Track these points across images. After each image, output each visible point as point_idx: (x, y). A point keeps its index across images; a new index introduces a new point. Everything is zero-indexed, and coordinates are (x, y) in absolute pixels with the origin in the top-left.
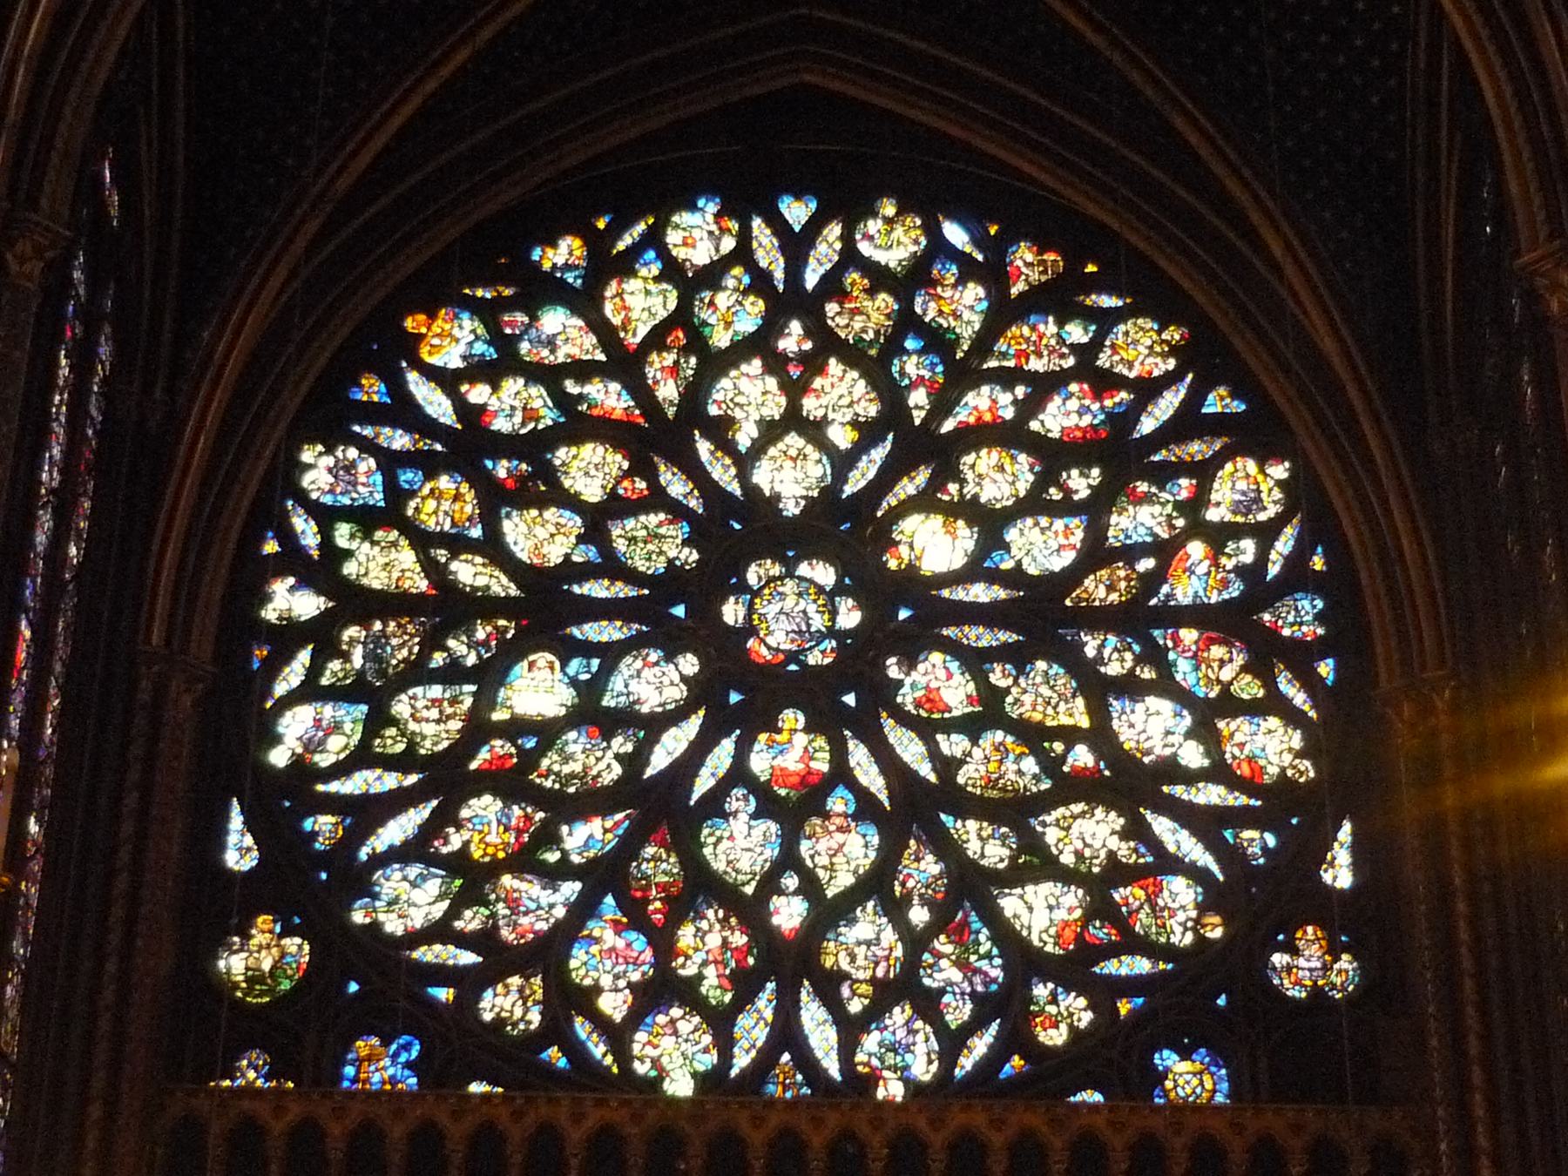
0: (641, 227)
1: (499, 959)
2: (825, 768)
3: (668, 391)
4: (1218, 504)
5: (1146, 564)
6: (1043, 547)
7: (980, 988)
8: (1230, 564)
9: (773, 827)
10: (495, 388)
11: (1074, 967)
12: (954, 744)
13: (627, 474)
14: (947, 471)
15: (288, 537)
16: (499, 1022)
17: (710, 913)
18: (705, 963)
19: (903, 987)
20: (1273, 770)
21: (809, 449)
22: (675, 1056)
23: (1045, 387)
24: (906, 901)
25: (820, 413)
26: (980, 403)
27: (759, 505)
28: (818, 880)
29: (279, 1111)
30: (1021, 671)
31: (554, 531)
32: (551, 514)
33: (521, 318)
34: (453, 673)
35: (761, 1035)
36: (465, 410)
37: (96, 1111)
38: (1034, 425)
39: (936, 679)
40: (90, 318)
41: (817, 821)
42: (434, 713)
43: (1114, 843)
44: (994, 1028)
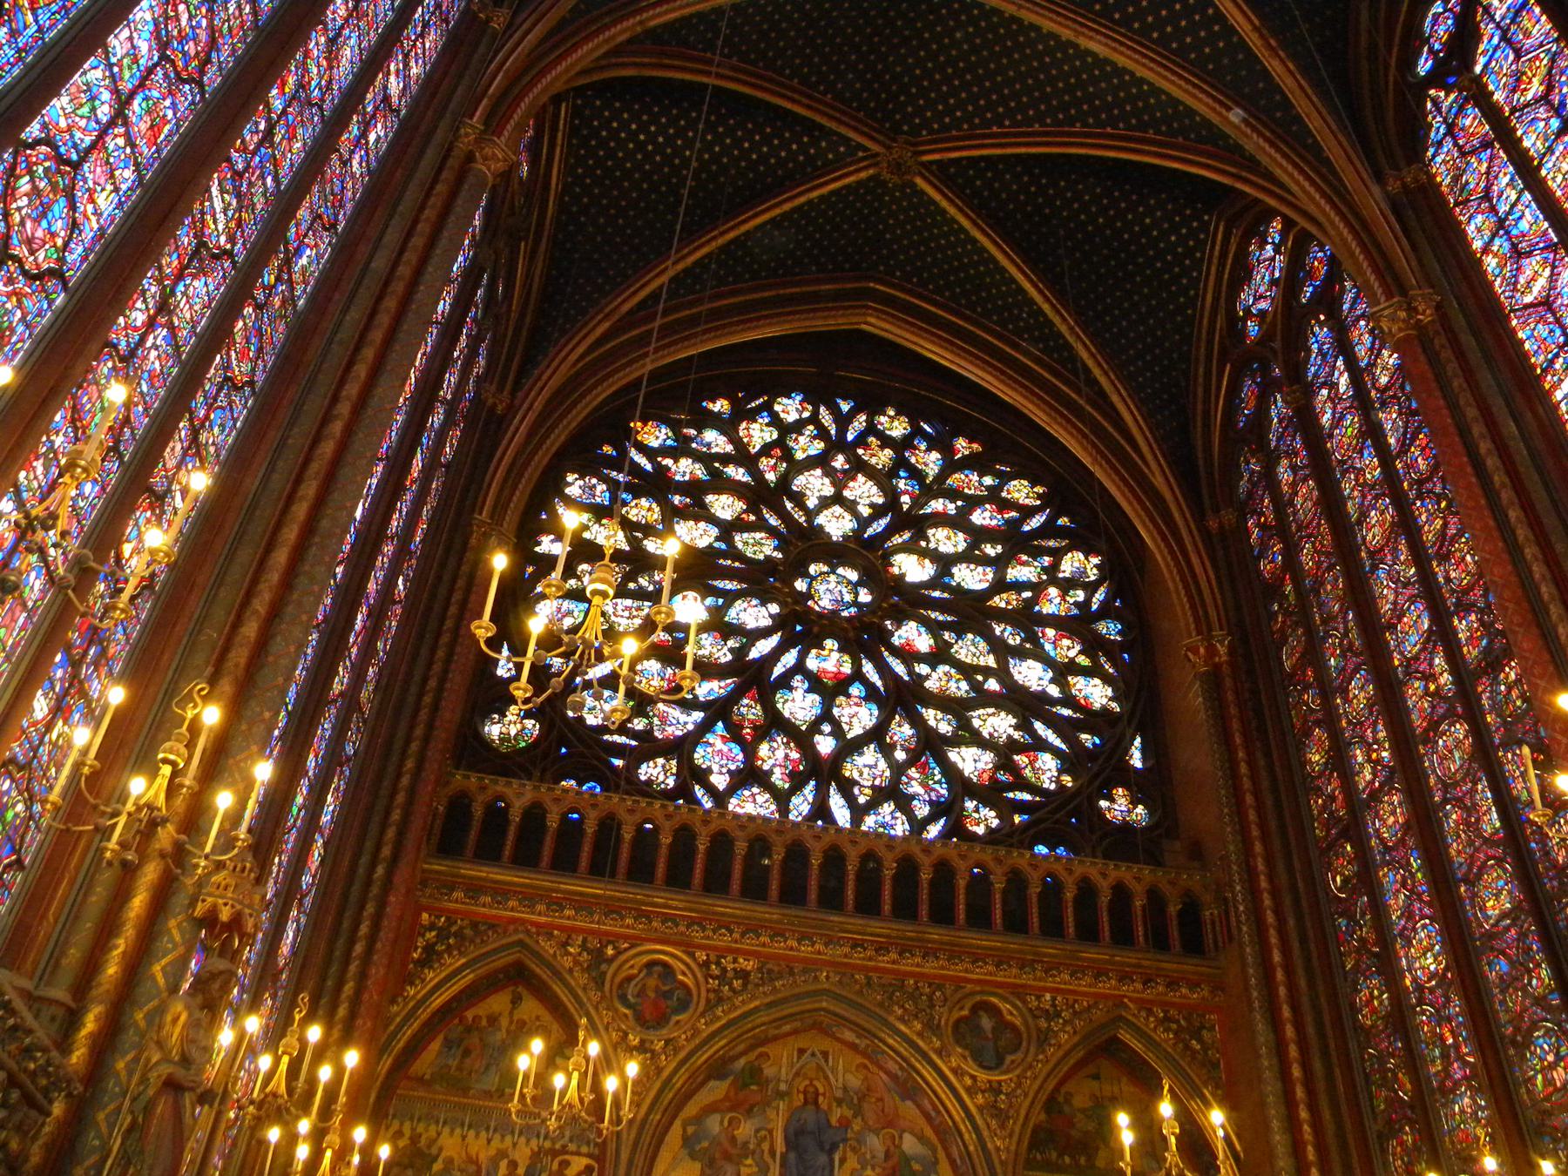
5: (1027, 594)
6: (971, 578)
9: (817, 698)
11: (989, 793)
12: (923, 669)
13: (745, 512)
16: (649, 782)
19: (891, 792)
23: (974, 502)
24: (893, 746)
26: (937, 505)
30: (960, 635)
32: (702, 525)
33: (693, 432)
35: (805, 809)
41: (842, 698)
42: (626, 614)
43: (1011, 731)
44: (942, 821)
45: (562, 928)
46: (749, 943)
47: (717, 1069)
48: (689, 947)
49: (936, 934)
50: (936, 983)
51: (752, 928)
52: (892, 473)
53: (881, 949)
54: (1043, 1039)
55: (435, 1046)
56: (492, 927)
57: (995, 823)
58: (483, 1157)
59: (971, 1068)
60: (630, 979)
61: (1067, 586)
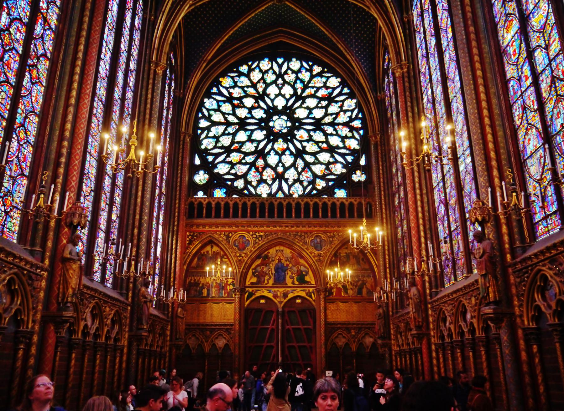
0: (256, 64)
1: (237, 177)
6: (318, 113)
11: (323, 177)
12: (305, 144)
13: (255, 103)
14: (304, 102)
15: (203, 114)
22: (264, 191)
27: (275, 108)
29: (205, 200)
32: (243, 109)
33: (238, 78)
34: (229, 134)
36: (229, 93)
37: (177, 201)
38: (317, 94)
39: (302, 134)
40: (170, 79)
45: (219, 231)
46: (262, 229)
47: (258, 257)
48: (248, 232)
49: (305, 221)
50: (306, 233)
51: (262, 225)
53: (292, 226)
54: (331, 242)
55: (196, 259)
56: (203, 233)
58: (210, 282)
59: (315, 251)
60: (236, 240)
61: (345, 111)
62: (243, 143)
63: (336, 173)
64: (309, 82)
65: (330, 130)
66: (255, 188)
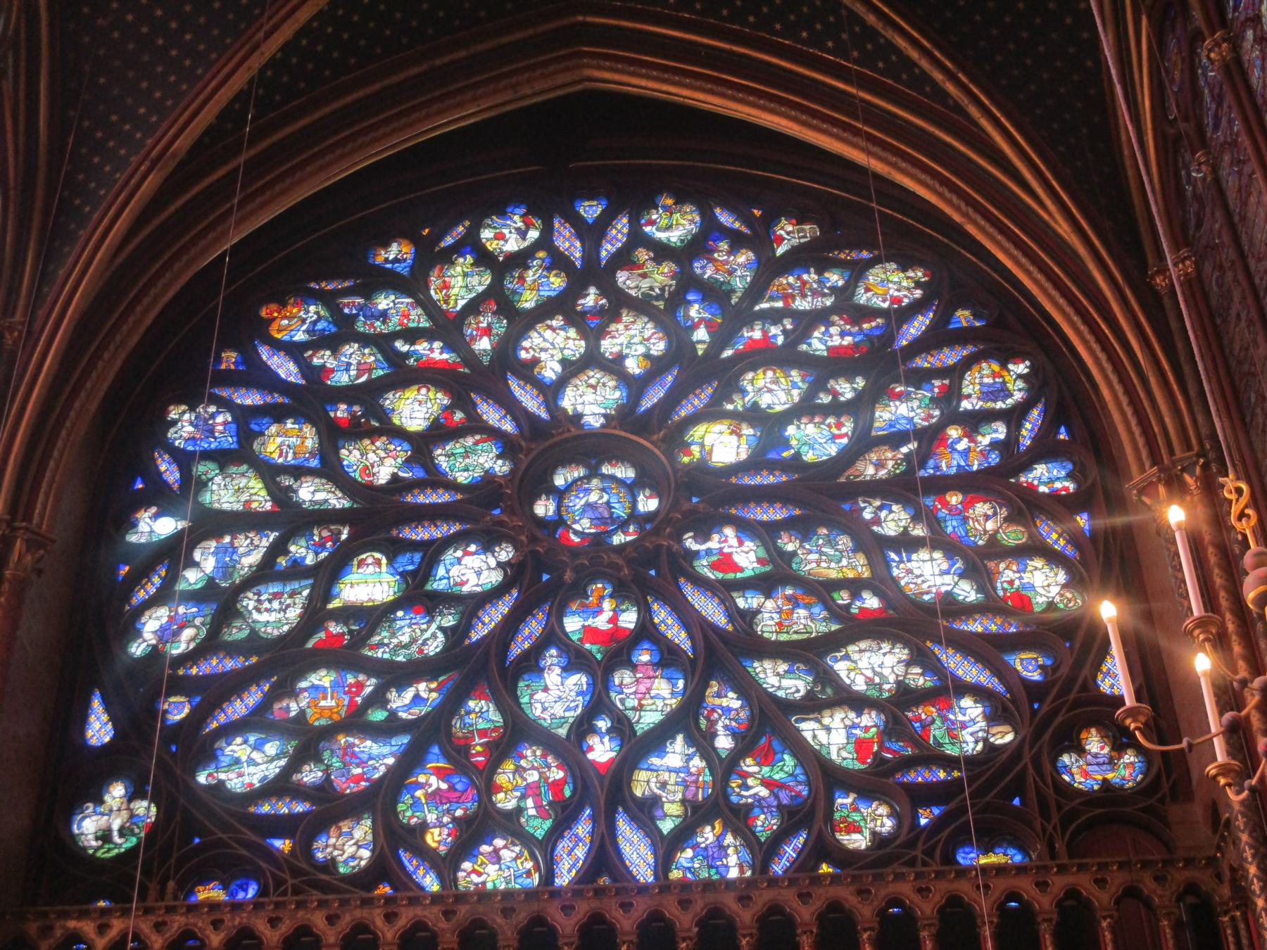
1: (331, 808)
2: (632, 626)
3: (484, 344)
4: (969, 396)
6: (815, 441)
7: (785, 802)
8: (985, 441)
10: (335, 352)
11: (874, 782)
14: (731, 387)
17: (529, 753)
18: (523, 797)
19: (715, 807)
20: (1041, 600)
21: (605, 380)
25: (616, 349)
28: (629, 720)
31: (383, 454)
36: (306, 368)
42: (276, 605)
52: (677, 300)
57: (887, 825)
61: (974, 422)
62: (372, 618)
63: (951, 750)
64: (757, 290)
65: (894, 520)
66: (446, 865)
